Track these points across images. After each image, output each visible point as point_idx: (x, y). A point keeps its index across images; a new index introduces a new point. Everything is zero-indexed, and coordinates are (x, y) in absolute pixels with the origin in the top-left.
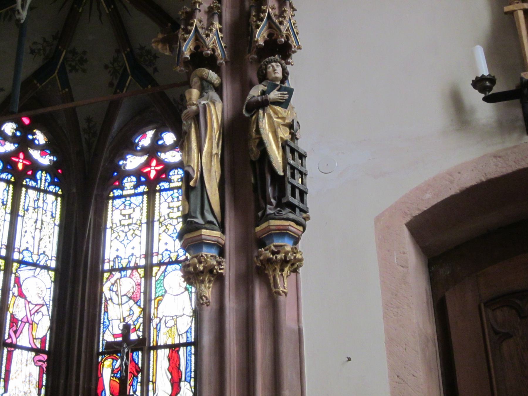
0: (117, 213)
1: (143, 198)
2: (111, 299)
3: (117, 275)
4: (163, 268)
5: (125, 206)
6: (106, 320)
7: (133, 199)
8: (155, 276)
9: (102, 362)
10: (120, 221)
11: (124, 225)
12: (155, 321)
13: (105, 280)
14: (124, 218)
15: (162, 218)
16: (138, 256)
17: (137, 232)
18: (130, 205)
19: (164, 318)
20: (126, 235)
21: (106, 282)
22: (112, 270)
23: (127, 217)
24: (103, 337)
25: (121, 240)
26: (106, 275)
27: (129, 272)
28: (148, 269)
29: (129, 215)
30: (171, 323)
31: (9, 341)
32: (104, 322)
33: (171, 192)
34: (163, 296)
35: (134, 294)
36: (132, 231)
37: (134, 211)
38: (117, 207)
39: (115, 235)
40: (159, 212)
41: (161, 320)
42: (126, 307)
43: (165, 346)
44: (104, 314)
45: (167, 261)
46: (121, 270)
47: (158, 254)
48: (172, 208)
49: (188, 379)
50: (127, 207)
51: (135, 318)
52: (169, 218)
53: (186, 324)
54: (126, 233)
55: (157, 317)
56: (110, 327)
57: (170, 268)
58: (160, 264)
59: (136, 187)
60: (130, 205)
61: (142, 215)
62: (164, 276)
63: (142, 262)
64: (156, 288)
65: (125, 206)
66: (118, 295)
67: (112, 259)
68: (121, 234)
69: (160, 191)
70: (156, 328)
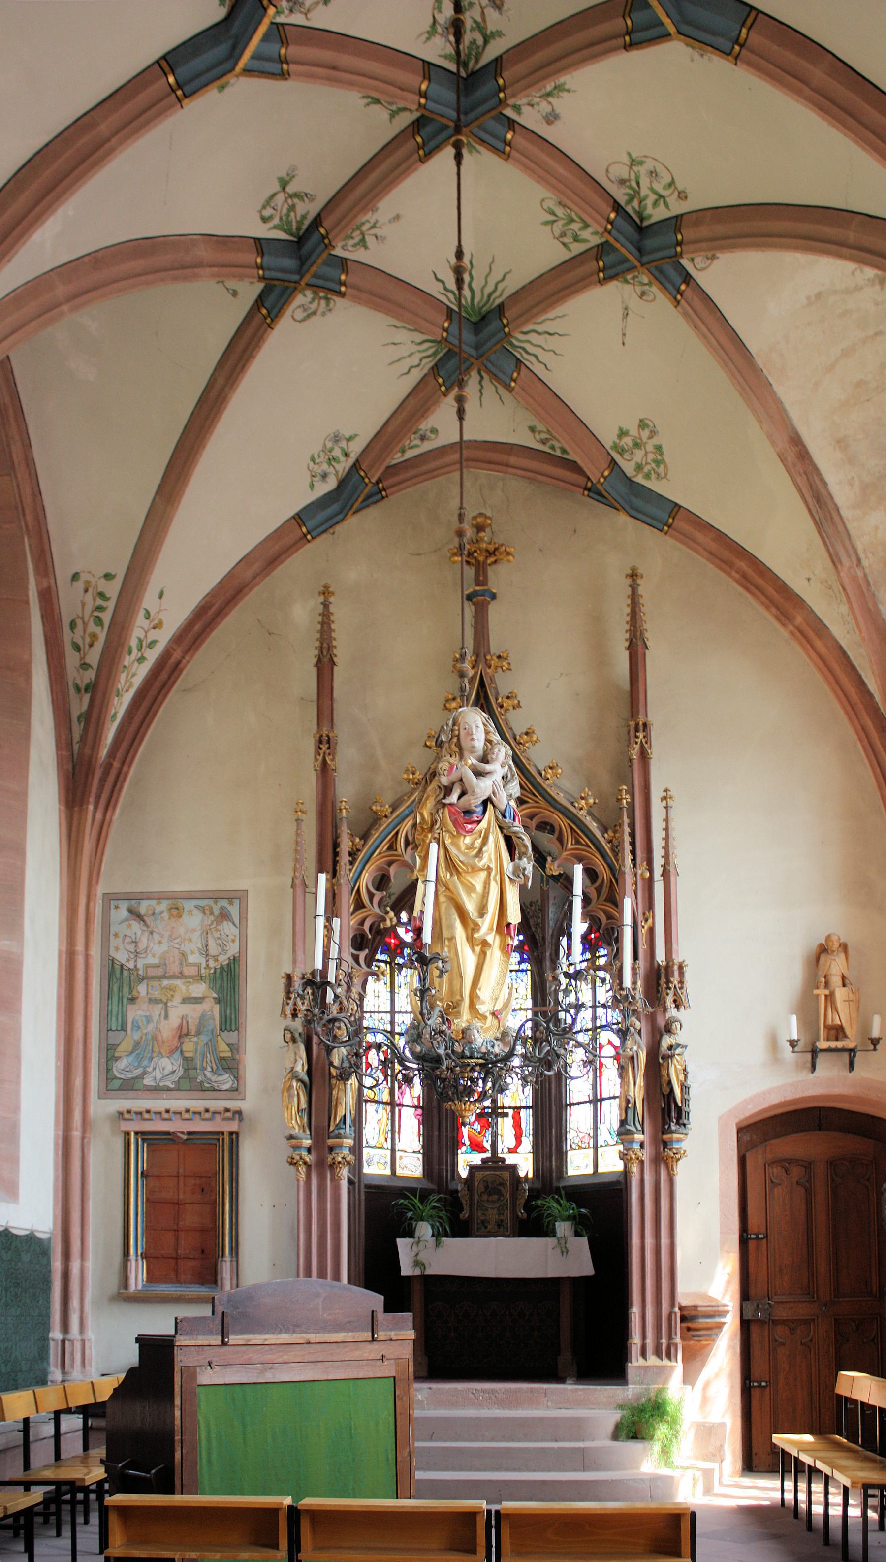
31: (398, 1102)
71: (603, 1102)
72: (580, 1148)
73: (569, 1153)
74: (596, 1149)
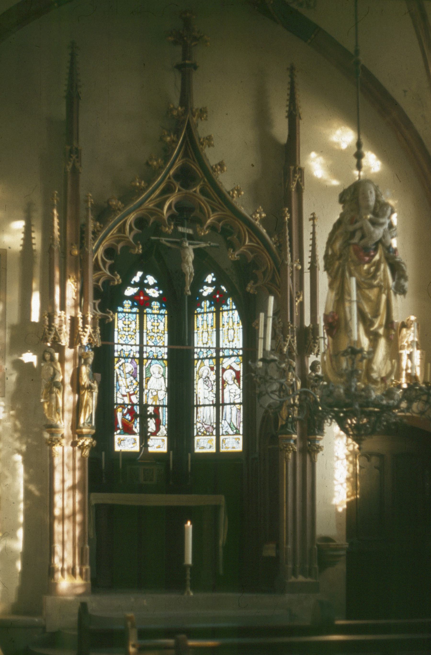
0: (120, 322)
1: (136, 317)
2: (120, 374)
3: (123, 361)
4: (149, 361)
5: (125, 319)
6: (117, 386)
7: (130, 315)
8: (145, 365)
9: (117, 409)
10: (123, 328)
11: (125, 331)
12: (146, 391)
13: (115, 363)
14: (125, 326)
15: (148, 332)
16: (135, 351)
17: (133, 336)
18: (128, 318)
19: (151, 390)
20: (127, 338)
21: (116, 364)
22: (119, 357)
23: (127, 326)
24: (116, 395)
26: (116, 360)
27: (130, 360)
28: (141, 360)
29: (128, 325)
30: (155, 393)
32: (116, 387)
33: (153, 316)
34: (150, 377)
37: (131, 323)
38: (120, 318)
39: (120, 336)
40: (147, 327)
41: (149, 390)
42: (128, 380)
43: (152, 405)
44: (117, 382)
45: (152, 357)
46: (125, 358)
47: (146, 352)
48: (154, 326)
49: (164, 424)
50: (127, 320)
51: (134, 387)
52: (152, 332)
53: (163, 397)
54: (127, 336)
55: (147, 389)
56: (120, 390)
57: (154, 362)
58: (148, 358)
59: (131, 308)
60: (128, 318)
61: (136, 326)
62: (150, 366)
63: (138, 355)
64: (146, 372)
65: (125, 319)
66: (123, 372)
67: (119, 350)
68: (123, 336)
69: (147, 314)
70: (147, 395)
71: (225, 407)
72: (205, 435)
73: (196, 438)
74: (218, 436)
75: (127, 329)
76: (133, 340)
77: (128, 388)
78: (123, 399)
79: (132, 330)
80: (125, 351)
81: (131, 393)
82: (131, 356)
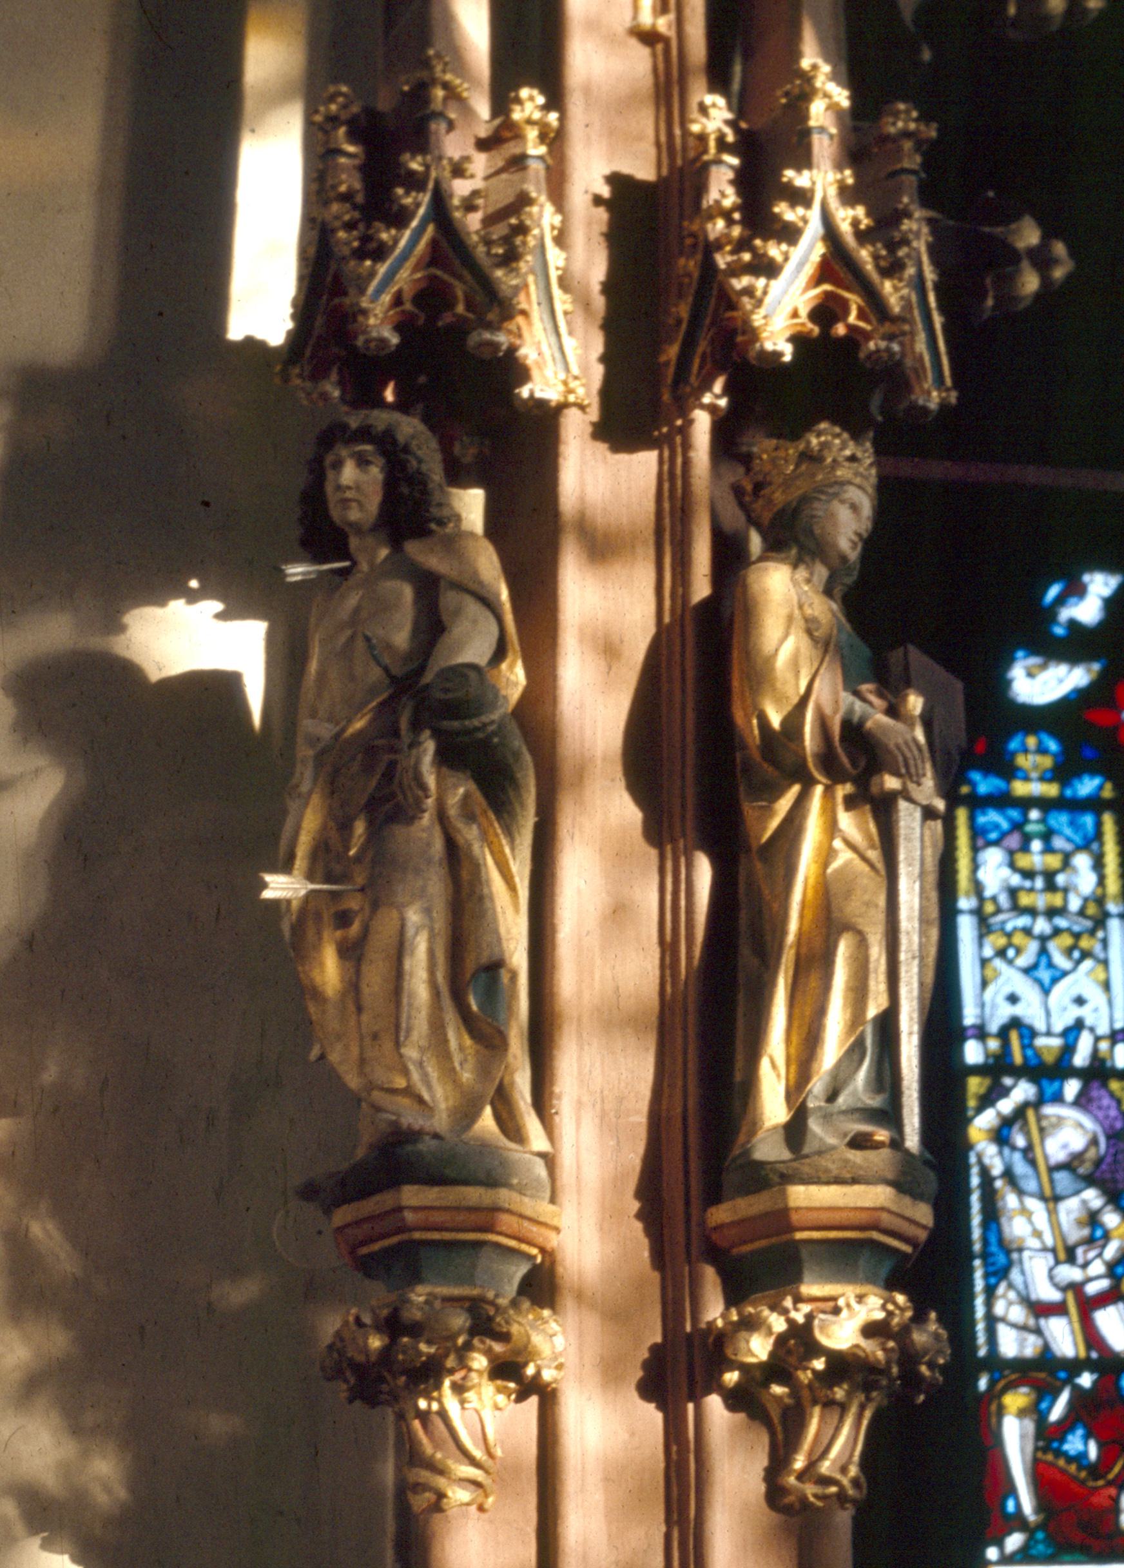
1: (1099, 825)
3: (1023, 1091)
11: (1032, 912)
14: (1027, 884)
20: (1043, 951)
21: (980, 1109)
23: (1039, 883)
25: (1023, 961)
26: (975, 1085)
29: (1049, 876)
35: (1104, 1167)
36: (1067, 940)
42: (1070, 1209)
50: (1036, 845)
56: (1015, 1275)
66: (1033, 1163)
67: (993, 1027)
68: (1018, 939)
75: (1041, 901)
76: (1088, 964)
77: (1071, 1258)
78: (1038, 1331)
79: (1074, 904)
80: (1033, 1033)
81: (1092, 1289)
82: (1081, 1058)
